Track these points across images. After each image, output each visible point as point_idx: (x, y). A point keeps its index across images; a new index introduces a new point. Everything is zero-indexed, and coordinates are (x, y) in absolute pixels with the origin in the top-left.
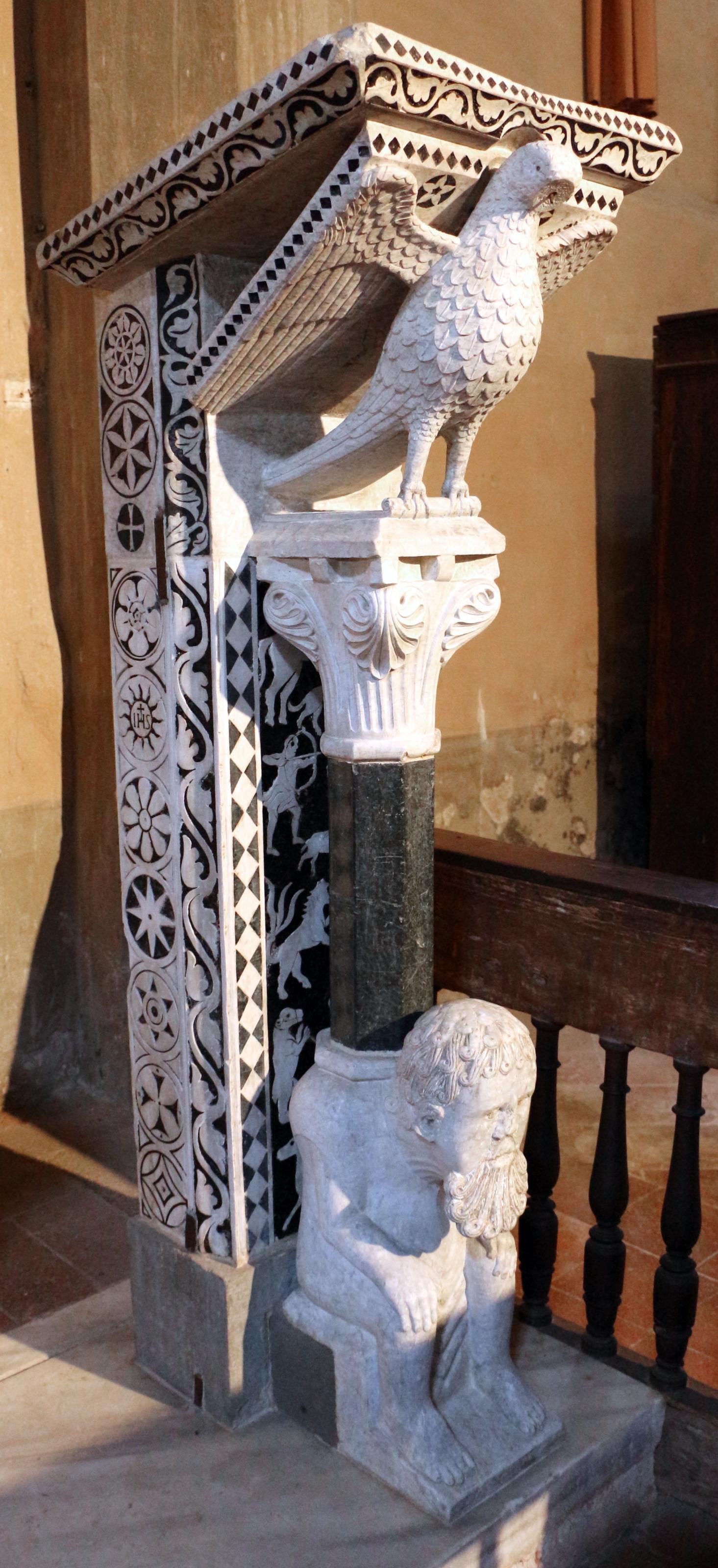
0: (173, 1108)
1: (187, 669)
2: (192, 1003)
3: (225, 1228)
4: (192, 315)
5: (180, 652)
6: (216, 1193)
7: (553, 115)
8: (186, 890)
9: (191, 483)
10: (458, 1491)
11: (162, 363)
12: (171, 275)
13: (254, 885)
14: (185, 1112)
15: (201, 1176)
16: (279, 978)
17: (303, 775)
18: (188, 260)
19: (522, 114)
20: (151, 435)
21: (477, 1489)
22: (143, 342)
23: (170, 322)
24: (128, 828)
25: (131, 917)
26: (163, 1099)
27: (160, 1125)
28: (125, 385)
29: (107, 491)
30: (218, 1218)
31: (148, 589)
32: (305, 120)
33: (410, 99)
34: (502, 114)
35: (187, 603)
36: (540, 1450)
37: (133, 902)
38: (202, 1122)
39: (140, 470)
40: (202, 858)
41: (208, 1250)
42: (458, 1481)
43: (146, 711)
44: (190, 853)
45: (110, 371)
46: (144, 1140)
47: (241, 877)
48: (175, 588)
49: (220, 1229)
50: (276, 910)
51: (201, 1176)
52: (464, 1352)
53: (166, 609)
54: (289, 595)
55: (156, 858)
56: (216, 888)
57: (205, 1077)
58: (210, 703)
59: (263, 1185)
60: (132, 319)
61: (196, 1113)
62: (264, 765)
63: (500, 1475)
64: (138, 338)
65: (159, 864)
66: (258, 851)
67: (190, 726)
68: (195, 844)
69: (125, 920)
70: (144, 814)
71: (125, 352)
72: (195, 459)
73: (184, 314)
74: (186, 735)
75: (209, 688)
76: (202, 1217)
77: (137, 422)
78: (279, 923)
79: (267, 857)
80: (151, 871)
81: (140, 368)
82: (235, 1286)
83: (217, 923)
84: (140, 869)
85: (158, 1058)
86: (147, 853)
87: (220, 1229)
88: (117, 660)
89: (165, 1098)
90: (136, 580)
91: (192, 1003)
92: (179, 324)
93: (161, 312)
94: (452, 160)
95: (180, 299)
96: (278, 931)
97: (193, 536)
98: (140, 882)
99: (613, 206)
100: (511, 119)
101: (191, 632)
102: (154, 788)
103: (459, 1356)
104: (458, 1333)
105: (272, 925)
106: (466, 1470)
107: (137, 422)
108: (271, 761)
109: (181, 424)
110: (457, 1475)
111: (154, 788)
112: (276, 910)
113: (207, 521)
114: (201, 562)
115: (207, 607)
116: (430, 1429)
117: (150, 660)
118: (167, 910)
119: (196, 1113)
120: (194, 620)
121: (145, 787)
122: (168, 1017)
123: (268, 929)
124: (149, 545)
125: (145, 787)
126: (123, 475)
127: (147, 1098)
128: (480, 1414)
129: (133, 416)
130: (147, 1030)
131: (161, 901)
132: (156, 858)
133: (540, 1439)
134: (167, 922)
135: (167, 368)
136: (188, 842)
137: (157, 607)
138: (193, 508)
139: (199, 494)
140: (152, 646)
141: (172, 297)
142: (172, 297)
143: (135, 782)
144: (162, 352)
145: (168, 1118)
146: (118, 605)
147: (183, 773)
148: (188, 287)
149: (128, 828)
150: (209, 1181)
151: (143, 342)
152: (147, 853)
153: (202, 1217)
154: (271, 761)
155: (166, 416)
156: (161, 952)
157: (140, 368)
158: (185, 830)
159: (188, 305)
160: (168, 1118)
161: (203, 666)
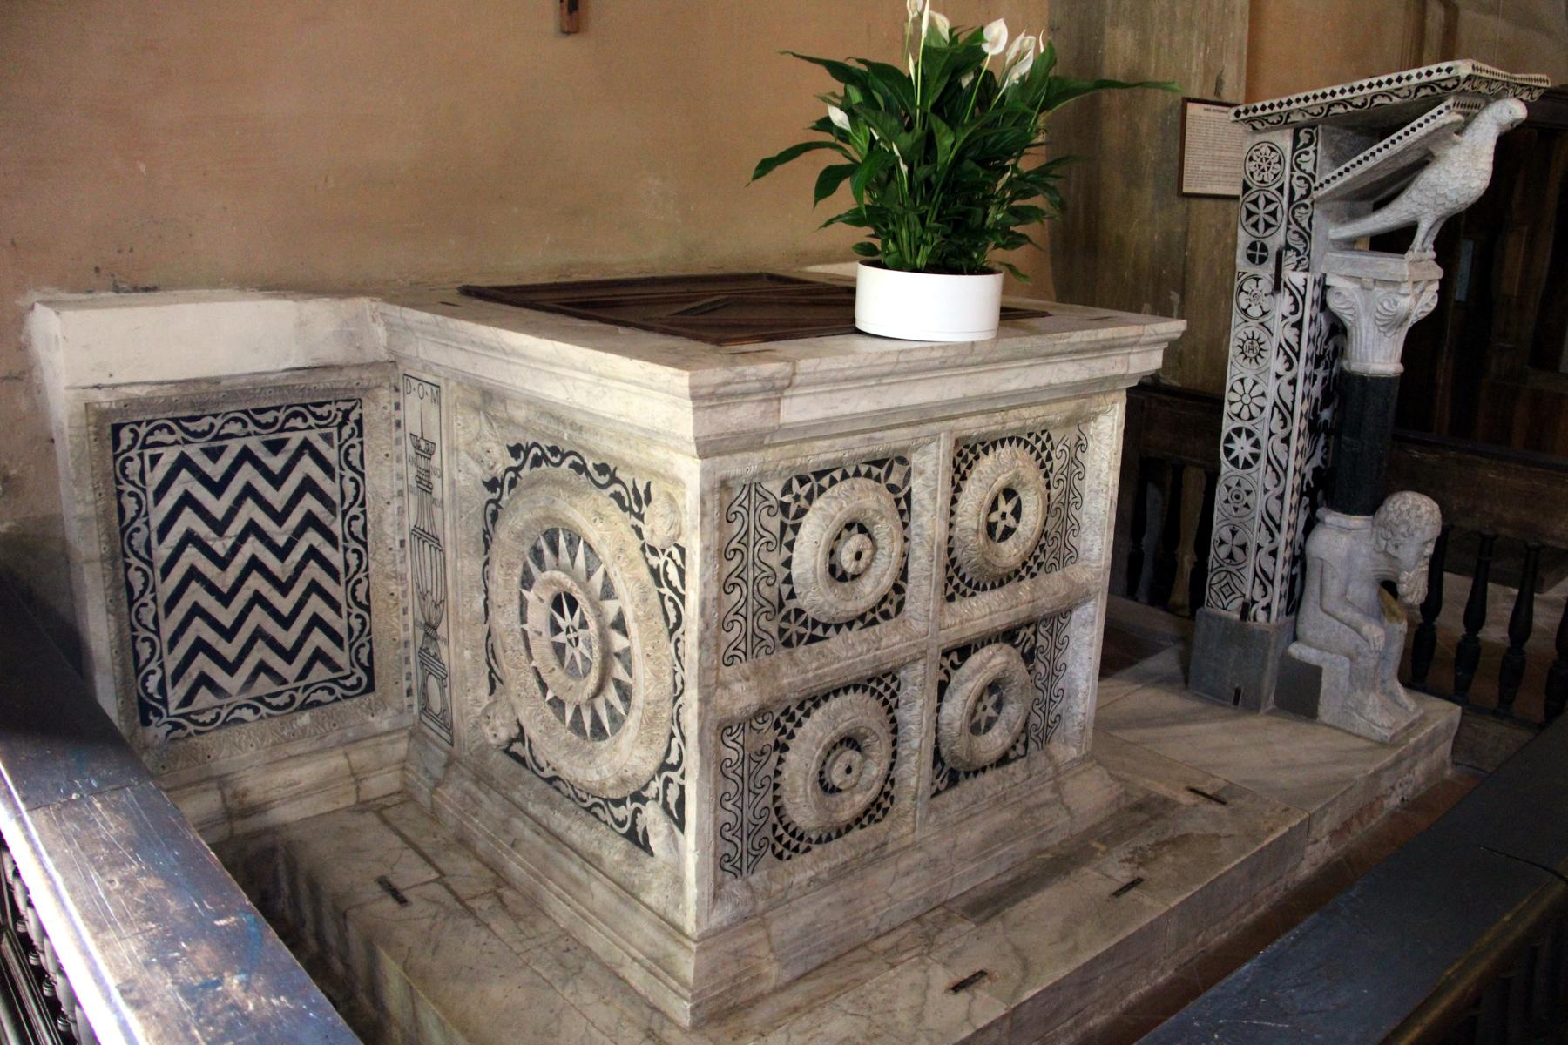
0: (1243, 547)
1: (1288, 326)
2: (1266, 491)
3: (1267, 608)
4: (1312, 154)
5: (1284, 317)
6: (1265, 589)
8: (1271, 434)
9: (1301, 236)
11: (1292, 176)
12: (1302, 134)
14: (1252, 548)
15: (1257, 580)
17: (1324, 379)
18: (1313, 128)
20: (1279, 209)
22: (1279, 162)
23: (1299, 156)
24: (1231, 403)
25: (1226, 449)
26: (1236, 542)
27: (1231, 556)
28: (1263, 182)
29: (1241, 232)
30: (1263, 602)
31: (1266, 285)
32: (1423, 92)
35: (1292, 294)
37: (1229, 439)
38: (1262, 553)
39: (1268, 226)
40: (1284, 419)
41: (1255, 619)
43: (1256, 344)
44: (1277, 416)
45: (1252, 173)
46: (1216, 565)
48: (1285, 285)
49: (1263, 609)
51: (1257, 580)
53: (1278, 296)
54: (1345, 293)
55: (1251, 418)
56: (1290, 434)
57: (1268, 528)
58: (1299, 343)
59: (1286, 586)
60: (1272, 150)
61: (1259, 547)
64: (1276, 160)
65: (1253, 422)
67: (1286, 353)
68: (1280, 411)
69: (1222, 450)
70: (1246, 396)
71: (1265, 165)
72: (1305, 224)
73: (1307, 153)
74: (1282, 358)
75: (1300, 337)
76: (1254, 602)
77: (1268, 202)
80: (1248, 425)
81: (1275, 176)
83: (1288, 452)
84: (1238, 424)
85: (1236, 521)
86: (1245, 414)
87: (1263, 609)
88: (1237, 318)
89: (1238, 540)
90: (1258, 279)
91: (1266, 491)
92: (1304, 157)
93: (1294, 150)
95: (1305, 146)
97: (1299, 261)
98: (1238, 431)
101: (1293, 308)
102: (1255, 383)
107: (1268, 202)
109: (1298, 206)
111: (1255, 383)
113: (1308, 255)
114: (1303, 275)
115: (1303, 298)
117: (1261, 320)
118: (1257, 444)
119: (1259, 547)
120: (1295, 302)
121: (1248, 384)
122: (1250, 499)
124: (1270, 265)
125: (1248, 384)
126: (1255, 225)
127: (1222, 542)
129: (1266, 198)
130: (1229, 508)
131: (1252, 440)
132: (1251, 418)
134: (1254, 450)
135: (1294, 179)
136: (1276, 410)
137: (1272, 294)
138: (1301, 249)
139: (1305, 241)
140: (1265, 313)
141: (1301, 144)
142: (1301, 144)
143: (1242, 380)
144: (1292, 170)
145: (1238, 553)
146: (1241, 290)
147: (1278, 376)
148: (1311, 141)
149: (1231, 403)
150: (1262, 583)
151: (1279, 162)
152: (1245, 414)
153: (1254, 602)
155: (1291, 202)
156: (1247, 465)
157: (1275, 176)
158: (1275, 404)
159: (1311, 149)
160: (1238, 553)
161: (1298, 325)
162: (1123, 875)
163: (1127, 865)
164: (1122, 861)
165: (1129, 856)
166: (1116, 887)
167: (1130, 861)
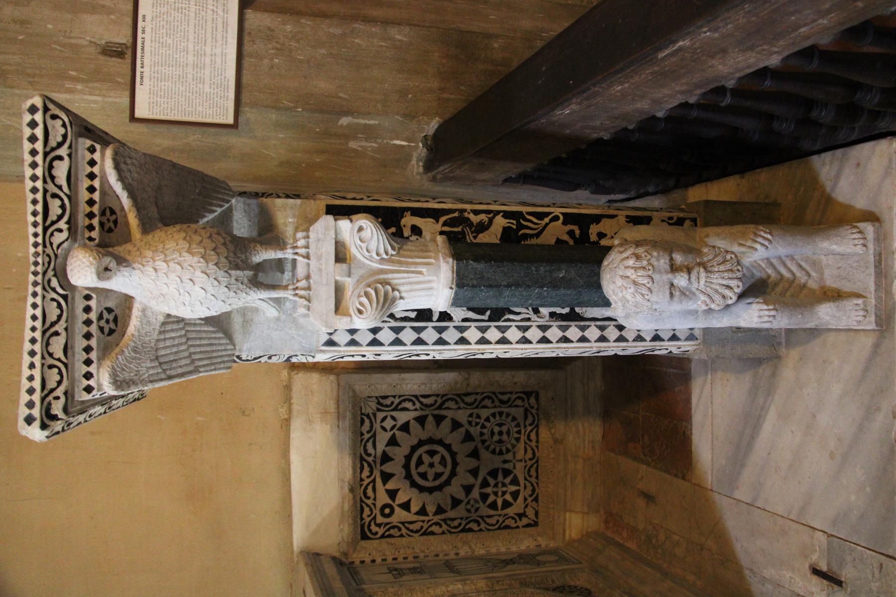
7: (44, 252)
10: (870, 317)
13: (503, 330)
16: (558, 312)
19: (49, 281)
21: (876, 305)
33: (59, 383)
34: (53, 300)
36: (877, 248)
42: (865, 314)
47: (497, 339)
50: (519, 313)
52: (802, 260)
62: (439, 320)
63: (876, 284)
66: (485, 326)
78: (528, 312)
79: (490, 319)
82: (711, 353)
94: (88, 322)
96: (532, 313)
99: (92, 150)
100: (54, 290)
103: (803, 264)
104: (789, 263)
105: (528, 316)
106: (862, 306)
108: (435, 317)
110: (862, 313)
112: (519, 313)
116: (830, 314)
123: (529, 319)
128: (840, 265)
133: (871, 246)
154: (435, 317)
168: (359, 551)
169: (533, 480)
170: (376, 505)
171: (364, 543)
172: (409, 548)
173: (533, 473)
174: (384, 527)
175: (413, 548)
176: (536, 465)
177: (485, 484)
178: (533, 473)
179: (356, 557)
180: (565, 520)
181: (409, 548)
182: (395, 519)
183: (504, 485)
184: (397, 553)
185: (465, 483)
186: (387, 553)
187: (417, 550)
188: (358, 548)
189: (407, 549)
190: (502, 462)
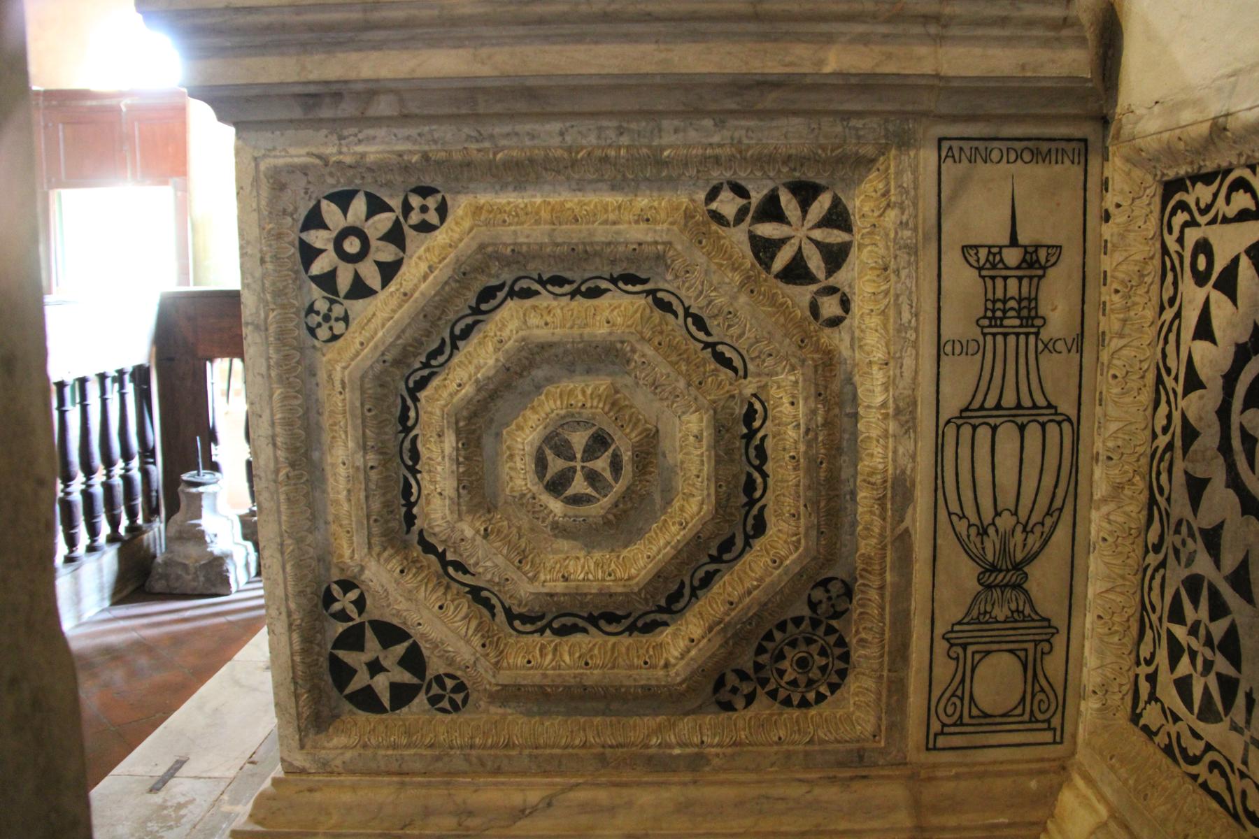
162: (180, 788)
163: (182, 800)
164: (192, 801)
165: (183, 812)
166: (184, 770)
167: (180, 806)
168: (1128, 174)
169: (1201, 769)
170: (1214, 227)
171: (1153, 191)
172: (1125, 321)
173: (1216, 783)
174: (1177, 252)
175: (1121, 336)
176: (1230, 805)
177: (1218, 609)
178: (1216, 783)
179: (1116, 170)
180: (1102, 797)
181: (1125, 321)
182: (1187, 284)
183: (1208, 666)
184: (1115, 286)
185: (1227, 537)
186: (1118, 257)
187: (1116, 343)
188: (1137, 173)
189: (1122, 316)
190: (1251, 689)
